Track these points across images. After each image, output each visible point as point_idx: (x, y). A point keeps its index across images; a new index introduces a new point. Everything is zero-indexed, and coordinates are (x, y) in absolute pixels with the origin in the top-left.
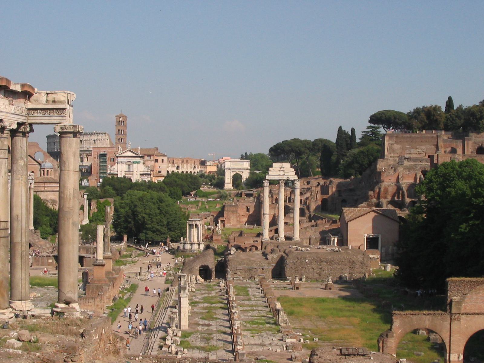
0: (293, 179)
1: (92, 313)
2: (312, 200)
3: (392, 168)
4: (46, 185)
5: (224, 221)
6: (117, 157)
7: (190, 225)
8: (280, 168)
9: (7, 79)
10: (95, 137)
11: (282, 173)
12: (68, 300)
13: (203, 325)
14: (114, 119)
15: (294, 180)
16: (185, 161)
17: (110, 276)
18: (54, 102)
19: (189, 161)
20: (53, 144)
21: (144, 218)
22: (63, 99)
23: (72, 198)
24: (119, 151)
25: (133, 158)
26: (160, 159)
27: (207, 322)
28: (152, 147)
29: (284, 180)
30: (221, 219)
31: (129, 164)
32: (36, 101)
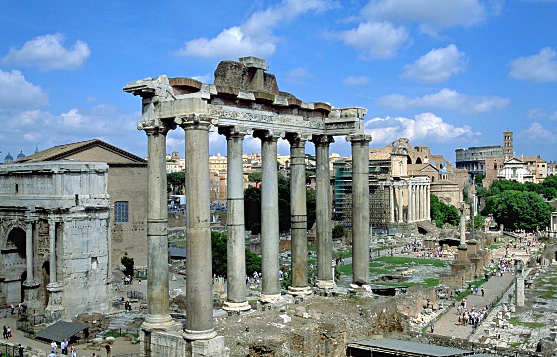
1: (448, 288)
6: (505, 164)
7: (554, 217)
9: (297, 100)
10: (492, 150)
12: (360, 282)
13: (539, 303)
17: (475, 258)
18: (346, 116)
20: (459, 156)
21: (516, 210)
22: (353, 113)
23: (361, 196)
26: (541, 165)
27: (543, 301)
31: (515, 169)
32: (333, 117)
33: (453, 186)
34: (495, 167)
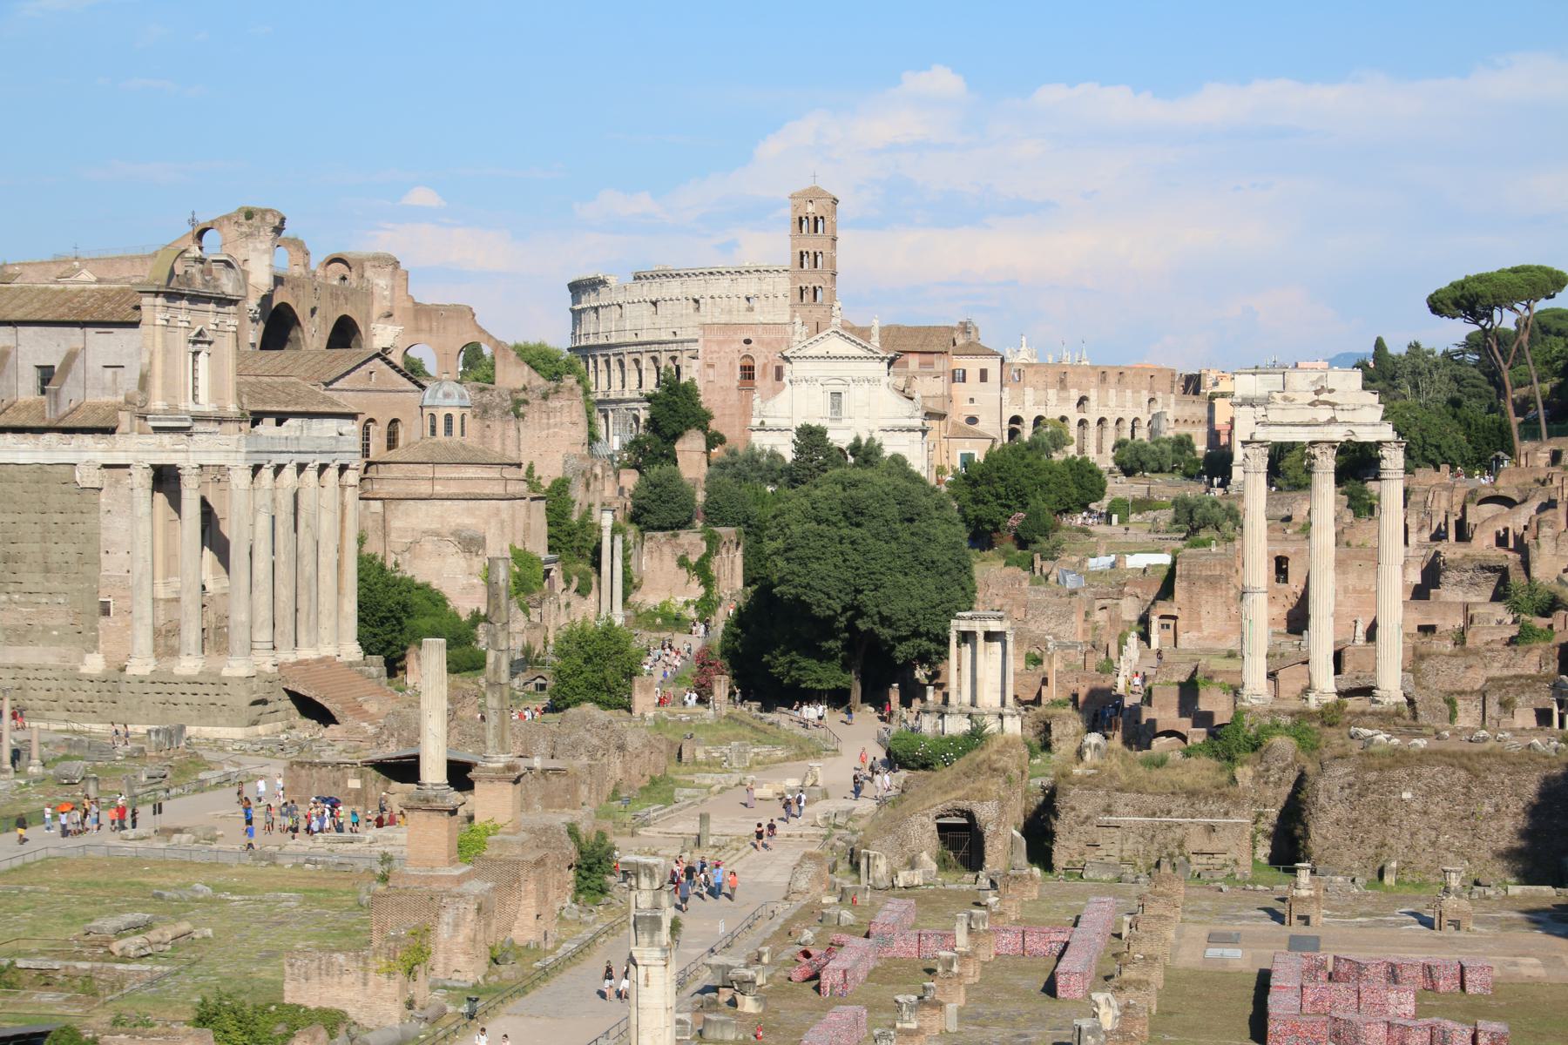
0: (1372, 438)
2: (1546, 531)
4: (442, 472)
5: (1175, 618)
8: (1317, 393)
10: (748, 286)
11: (1324, 414)
14: (788, 213)
15: (1379, 444)
16: (1112, 379)
19: (1128, 379)
24: (797, 338)
25: (852, 365)
26: (972, 365)
28: (951, 317)
29: (1331, 443)
30: (1164, 608)
33: (494, 473)
34: (748, 372)
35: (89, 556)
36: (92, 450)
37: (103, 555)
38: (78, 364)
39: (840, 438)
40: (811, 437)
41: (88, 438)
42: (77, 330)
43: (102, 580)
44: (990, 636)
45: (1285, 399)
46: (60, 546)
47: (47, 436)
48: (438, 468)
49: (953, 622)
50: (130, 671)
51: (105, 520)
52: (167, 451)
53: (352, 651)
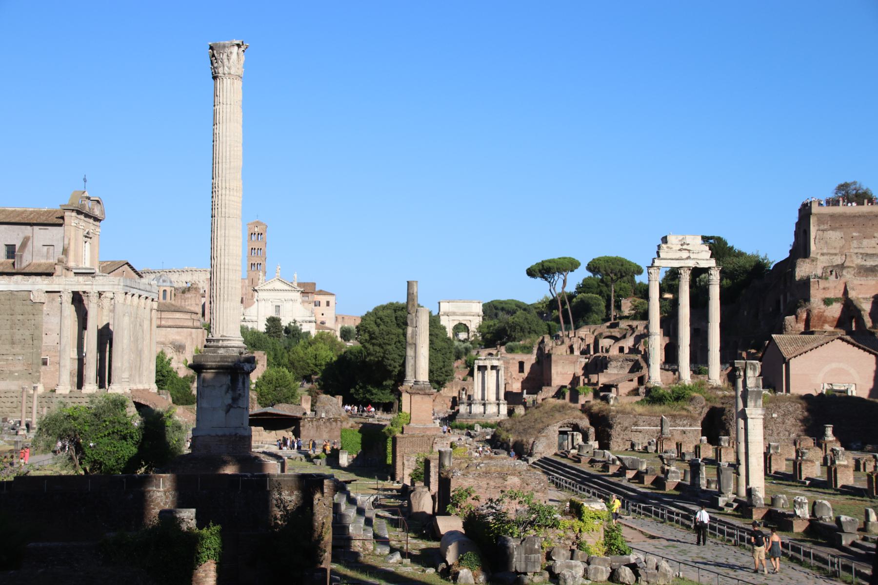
3: (831, 272)
11: (685, 254)
15: (710, 268)
25: (285, 293)
26: (323, 299)
29: (689, 268)
33: (188, 316)
35: (35, 338)
36: (39, 285)
37: (44, 335)
38: (30, 243)
39: (284, 323)
40: (273, 322)
41: (38, 278)
42: (29, 227)
43: (44, 348)
44: (493, 368)
45: (668, 247)
46: (21, 331)
47: (16, 277)
48: (163, 313)
49: (476, 361)
50: (58, 392)
51: (45, 319)
52: (80, 285)
53: (154, 388)
